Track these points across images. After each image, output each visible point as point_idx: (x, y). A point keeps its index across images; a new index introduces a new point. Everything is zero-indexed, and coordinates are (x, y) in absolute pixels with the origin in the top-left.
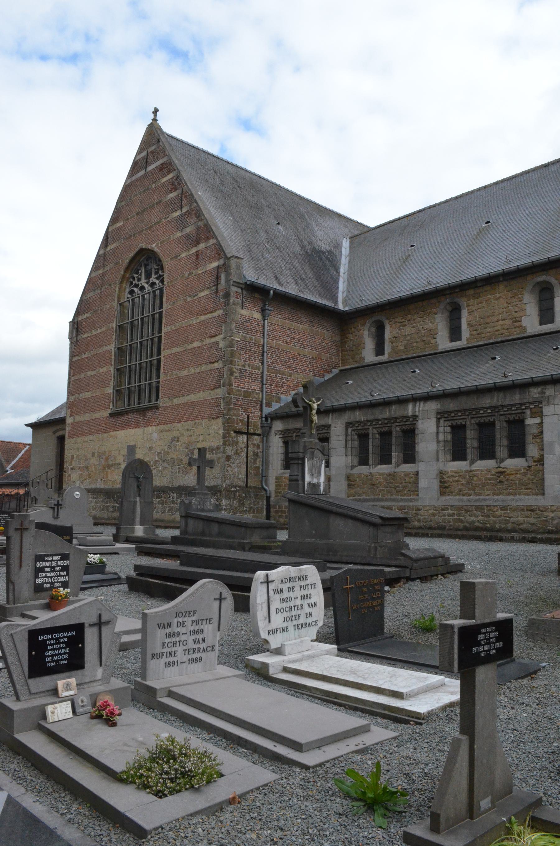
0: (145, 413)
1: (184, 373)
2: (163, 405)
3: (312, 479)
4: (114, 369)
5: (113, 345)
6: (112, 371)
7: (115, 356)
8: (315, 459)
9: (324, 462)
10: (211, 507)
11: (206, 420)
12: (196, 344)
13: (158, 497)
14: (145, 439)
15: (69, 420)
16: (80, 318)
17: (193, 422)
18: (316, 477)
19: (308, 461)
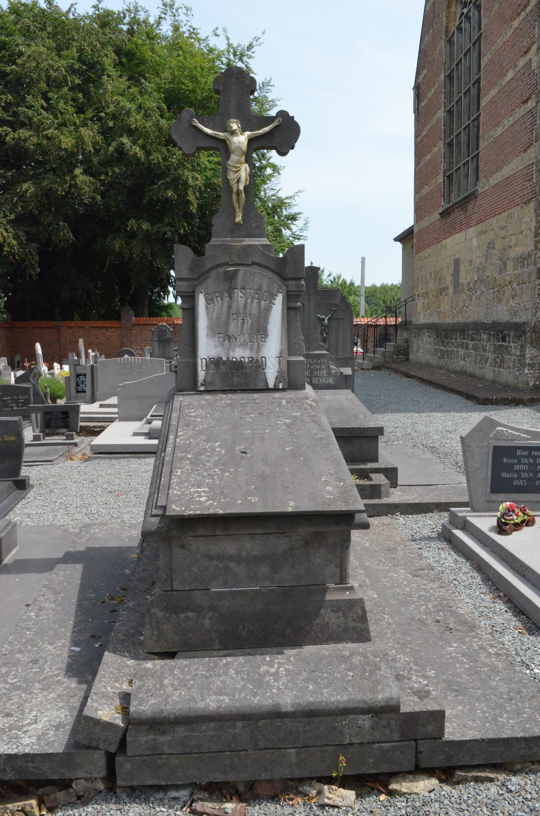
0: (466, 208)
1: (500, 130)
2: (483, 190)
3: (230, 348)
4: (445, 144)
5: (442, 109)
6: (442, 150)
7: (444, 126)
8: (238, 294)
9: (279, 301)
10: (331, 381)
11: (517, 208)
12: (510, 74)
13: (473, 340)
14: (467, 248)
15: (415, 231)
16: (421, 78)
17: (504, 215)
18: (244, 345)
19: (209, 301)
